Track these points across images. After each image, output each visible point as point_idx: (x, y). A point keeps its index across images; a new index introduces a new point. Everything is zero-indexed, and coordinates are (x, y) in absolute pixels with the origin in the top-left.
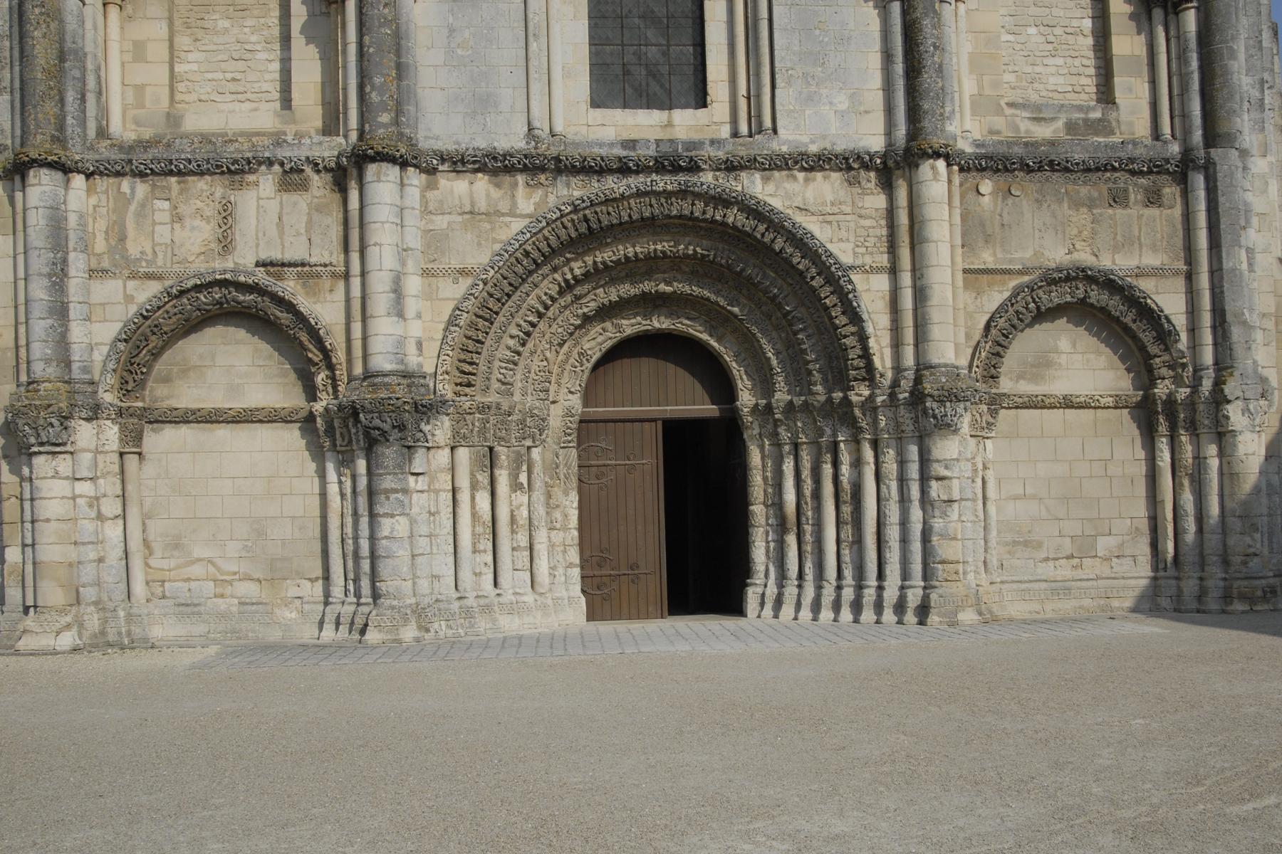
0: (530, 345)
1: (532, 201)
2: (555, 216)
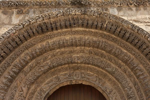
0: (14, 84)
1: (19, 19)
2: (26, 24)
